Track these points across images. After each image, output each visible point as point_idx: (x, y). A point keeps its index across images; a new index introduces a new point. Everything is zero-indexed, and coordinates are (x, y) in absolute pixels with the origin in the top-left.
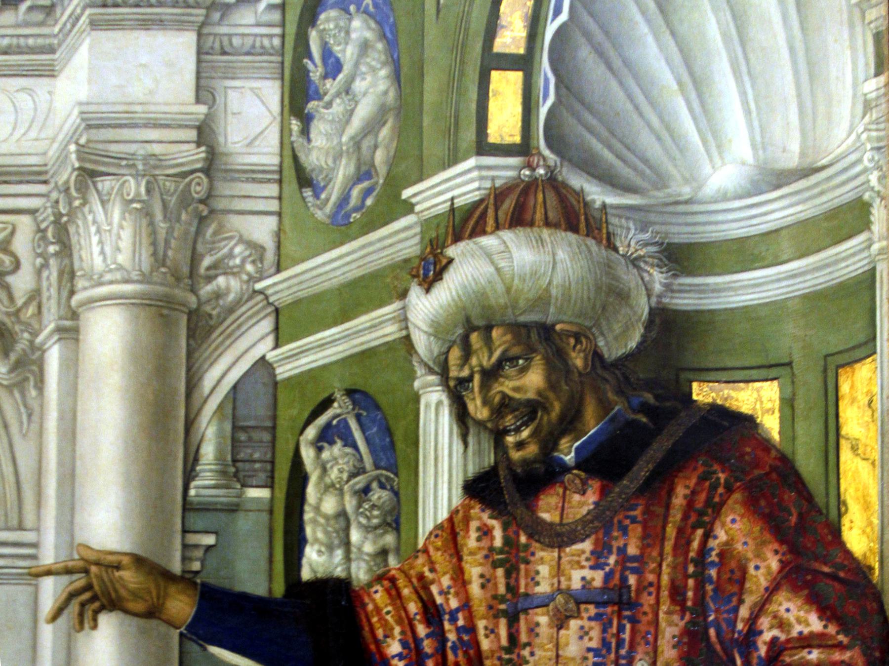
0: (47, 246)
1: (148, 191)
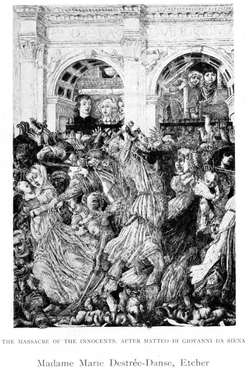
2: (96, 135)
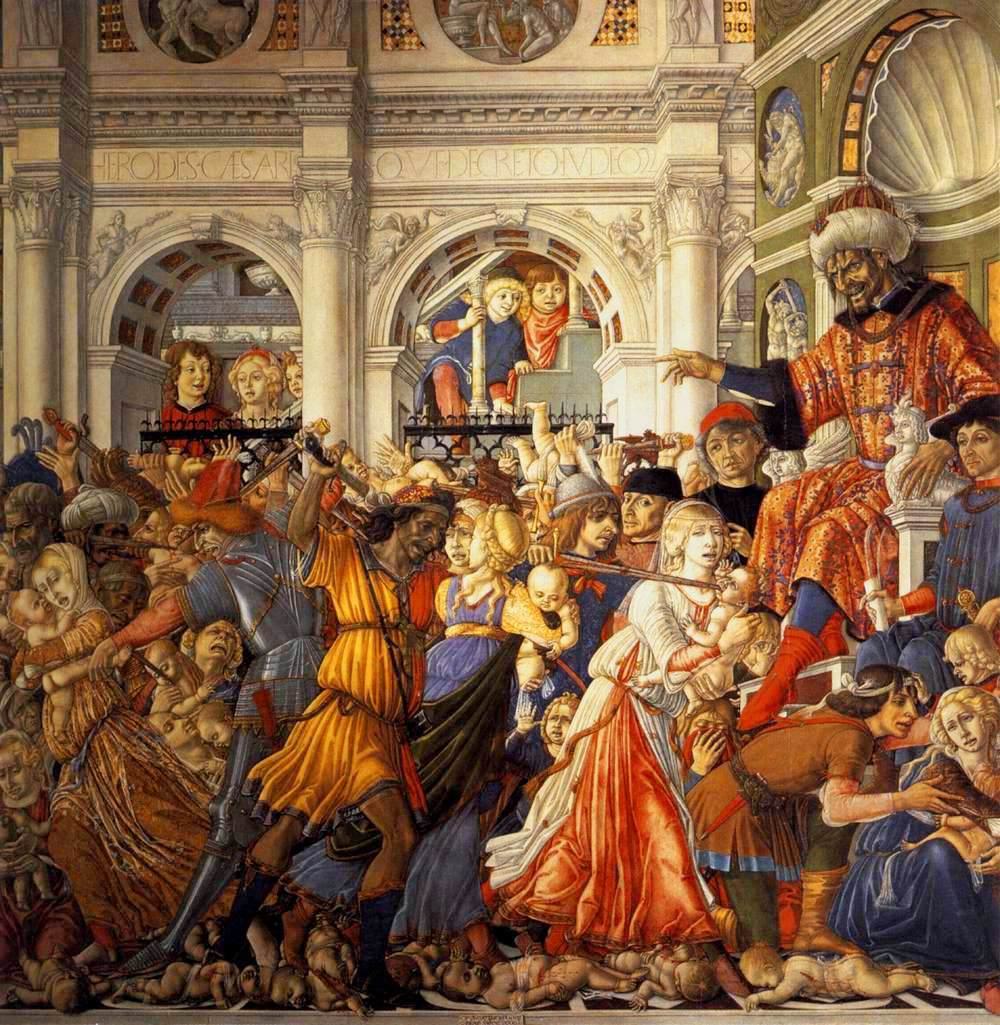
2: (220, 457)
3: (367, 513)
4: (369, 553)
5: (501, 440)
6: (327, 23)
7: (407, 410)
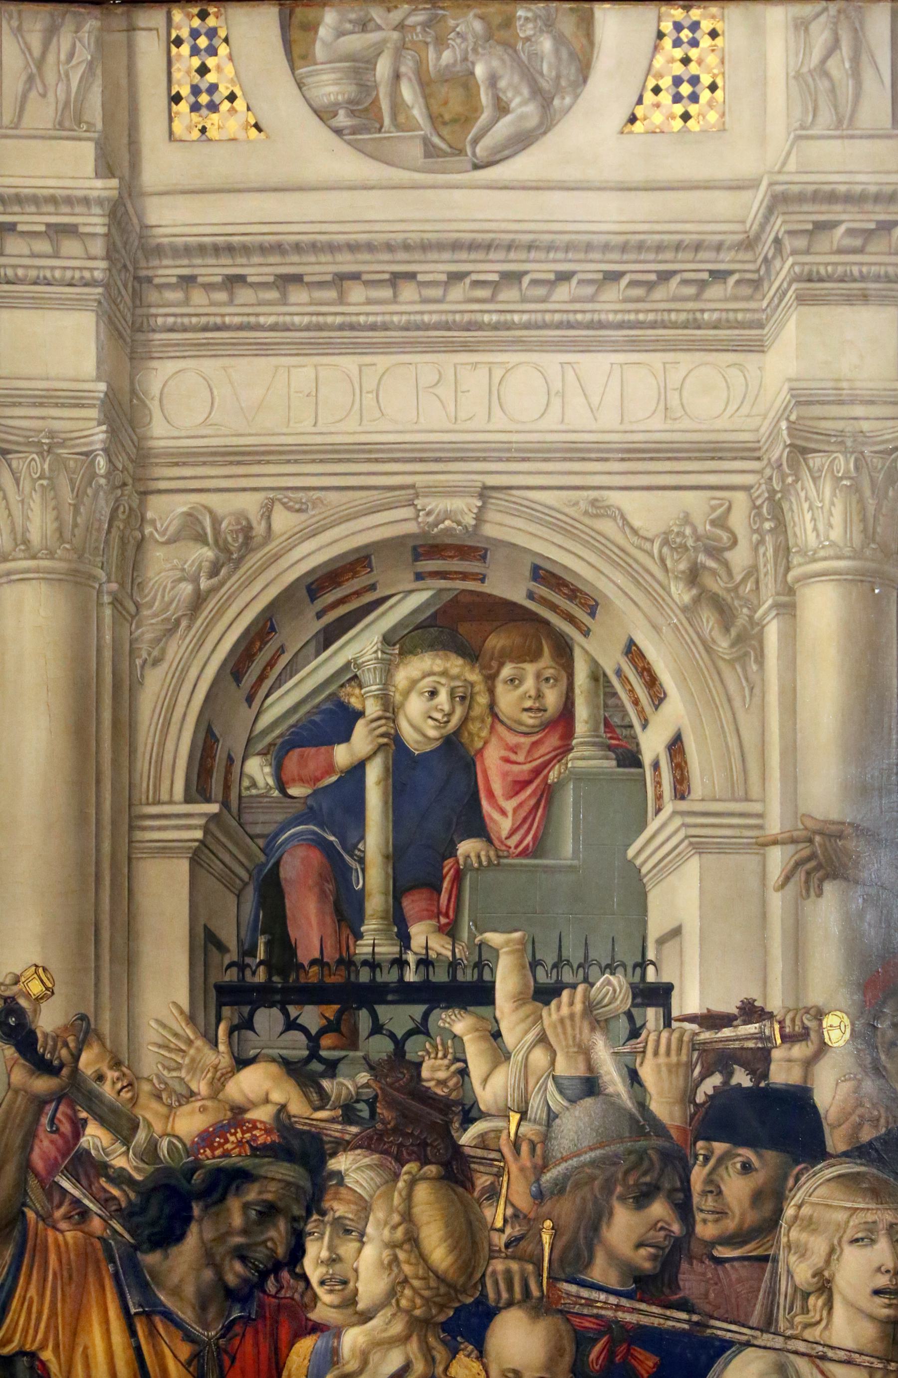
0: (762, 523)
1: (857, 468)
3: (131, 1182)
4: (134, 1268)
5: (426, 1016)
6: (51, 76)
7: (222, 948)
